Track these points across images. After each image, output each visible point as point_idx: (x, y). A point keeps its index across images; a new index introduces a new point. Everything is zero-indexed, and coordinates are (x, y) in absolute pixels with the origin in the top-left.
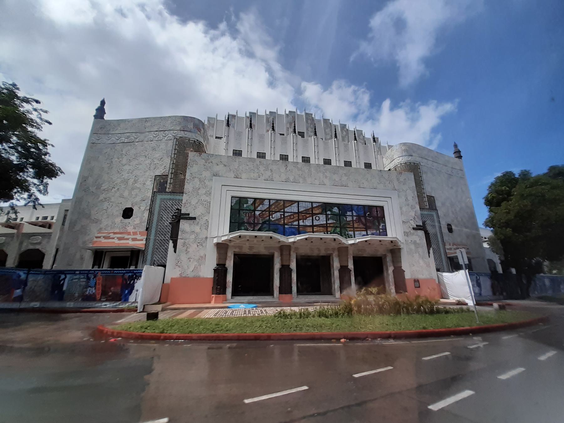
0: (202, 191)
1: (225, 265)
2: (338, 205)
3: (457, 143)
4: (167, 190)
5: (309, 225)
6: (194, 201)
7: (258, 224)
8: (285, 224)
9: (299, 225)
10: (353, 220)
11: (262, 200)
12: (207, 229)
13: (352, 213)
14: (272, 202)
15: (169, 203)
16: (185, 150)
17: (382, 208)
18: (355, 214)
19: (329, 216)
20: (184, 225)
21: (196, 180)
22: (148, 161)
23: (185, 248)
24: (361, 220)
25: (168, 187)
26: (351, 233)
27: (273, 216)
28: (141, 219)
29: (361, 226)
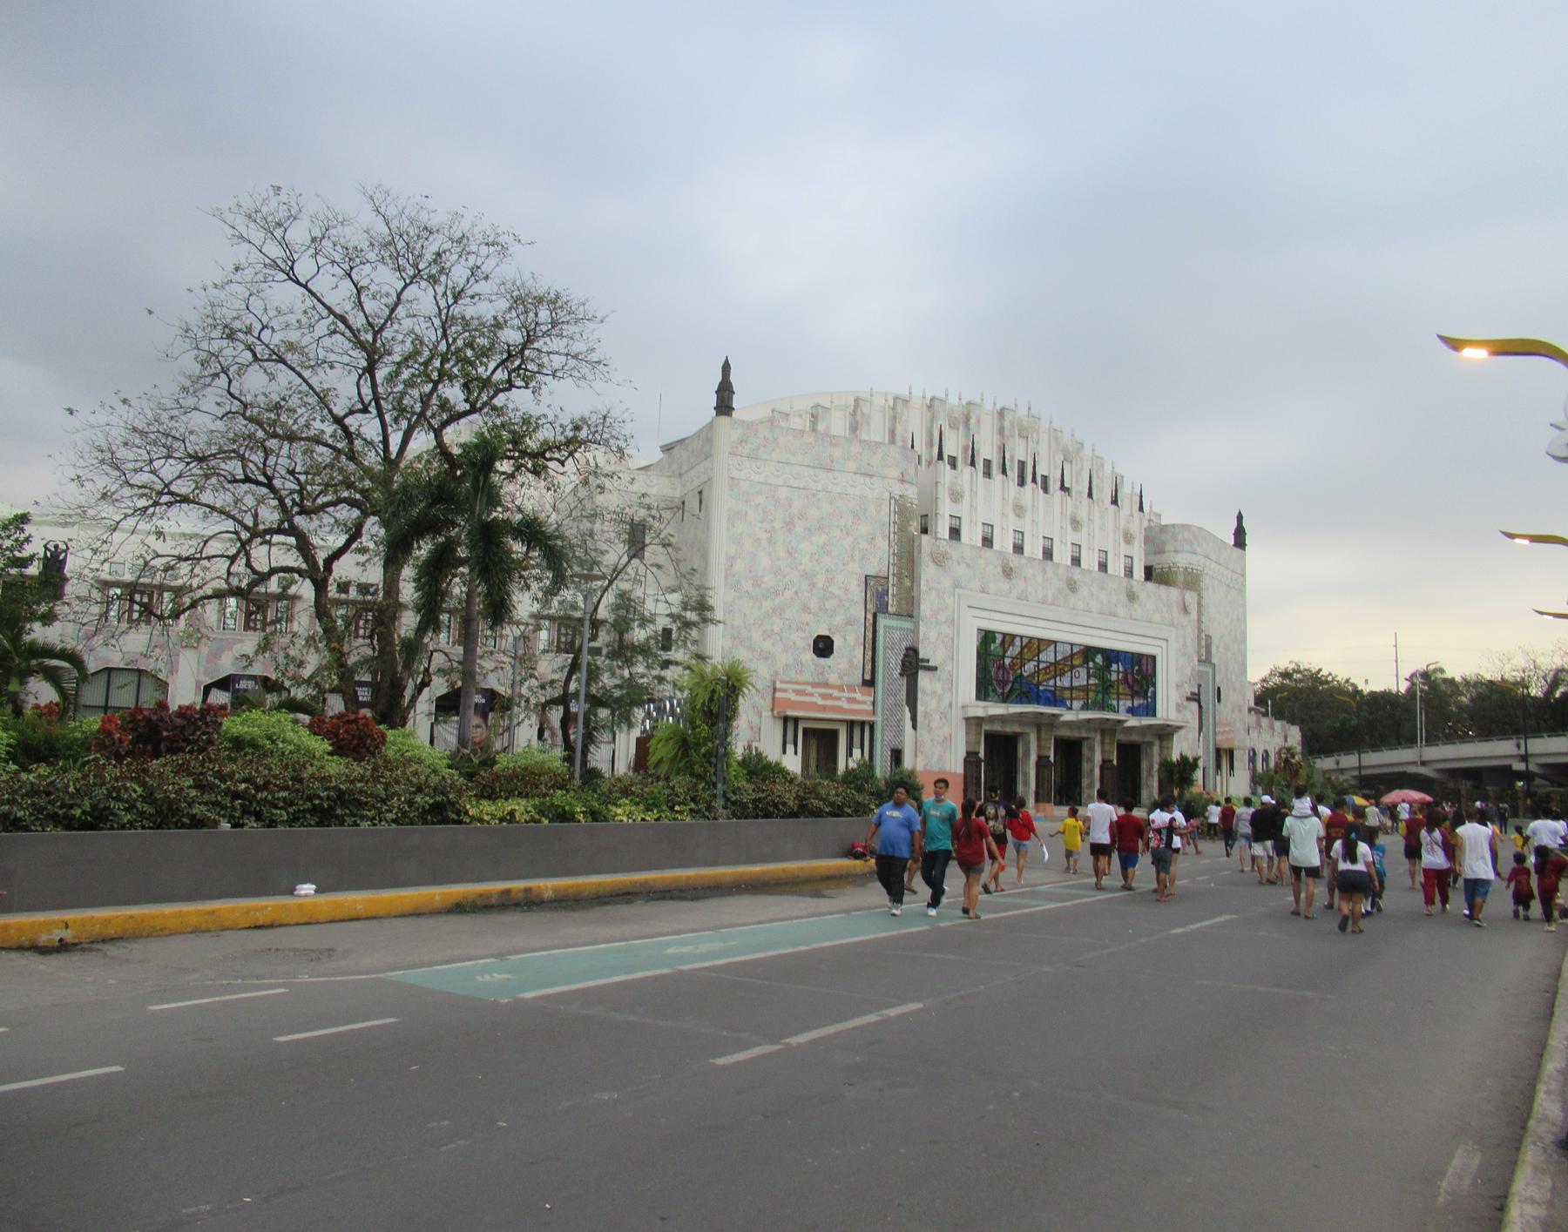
0: (943, 616)
6: (933, 636)
8: (1039, 683)
11: (1013, 636)
12: (951, 690)
14: (1025, 641)
15: (897, 634)
17: (1154, 658)
20: (924, 679)
22: (848, 542)
28: (851, 662)
29: (1128, 691)
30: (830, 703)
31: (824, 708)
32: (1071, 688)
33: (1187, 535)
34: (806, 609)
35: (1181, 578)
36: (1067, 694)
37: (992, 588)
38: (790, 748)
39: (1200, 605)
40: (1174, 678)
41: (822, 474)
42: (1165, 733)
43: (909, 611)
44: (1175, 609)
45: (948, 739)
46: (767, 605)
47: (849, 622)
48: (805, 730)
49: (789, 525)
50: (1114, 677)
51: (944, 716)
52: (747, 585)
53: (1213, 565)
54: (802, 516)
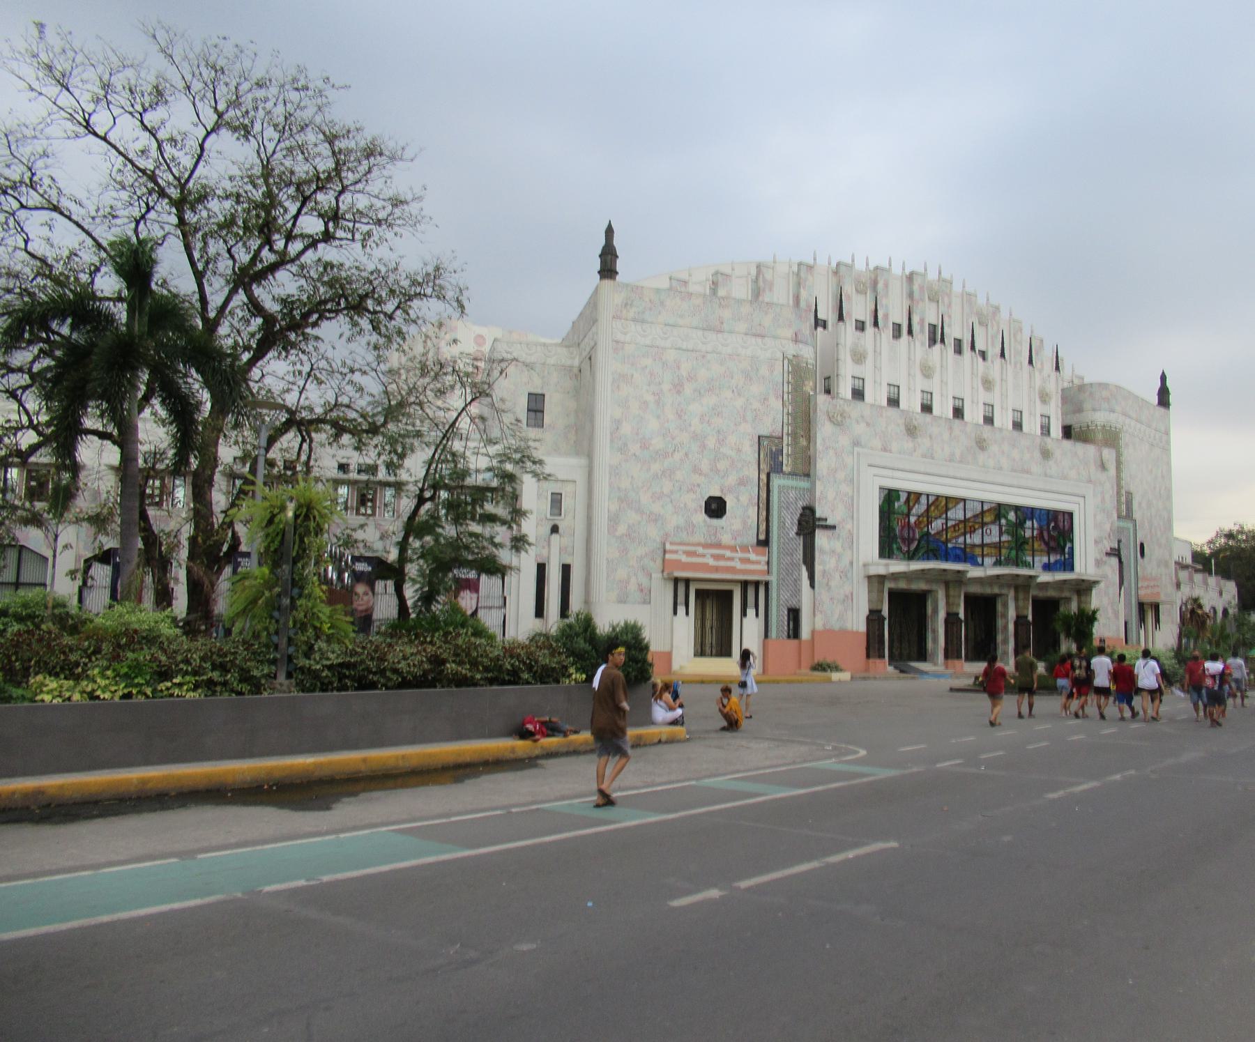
0: (841, 475)
2: (1017, 508)
4: (784, 468)
6: (831, 495)
7: (913, 539)
8: (947, 541)
11: (918, 495)
12: (851, 547)
14: (932, 499)
15: (792, 494)
18: (1036, 525)
20: (821, 538)
21: (831, 452)
22: (739, 403)
23: (825, 581)
25: (785, 462)
26: (1029, 559)
28: (744, 523)
29: (1043, 547)
30: (722, 563)
31: (717, 569)
32: (983, 545)
33: (1105, 393)
34: (696, 470)
35: (1100, 436)
36: (978, 551)
37: (895, 446)
38: (681, 609)
39: (1119, 464)
40: (1092, 534)
41: (711, 336)
42: (1083, 588)
43: (806, 470)
44: (1093, 469)
45: (849, 598)
46: (656, 467)
47: (742, 482)
48: (698, 592)
49: (678, 387)
50: (1028, 534)
51: (845, 574)
52: (634, 448)
53: (1133, 423)
54: (691, 378)
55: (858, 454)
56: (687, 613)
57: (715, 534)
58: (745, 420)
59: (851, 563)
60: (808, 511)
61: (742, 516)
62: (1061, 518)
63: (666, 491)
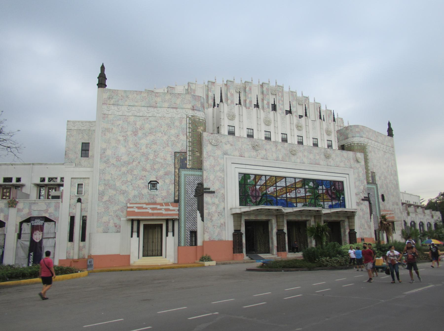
0: (217, 168)
1: (240, 230)
2: (313, 181)
3: (390, 122)
4: (188, 166)
5: (293, 197)
6: (212, 177)
7: (259, 196)
8: (277, 197)
9: (287, 197)
10: (323, 193)
11: (260, 176)
12: (224, 201)
13: (323, 187)
14: (268, 178)
15: (192, 178)
16: (197, 129)
17: (342, 182)
18: (324, 188)
19: (307, 190)
20: (207, 198)
21: (212, 158)
22: (165, 138)
23: (210, 217)
24: (328, 193)
25: (188, 163)
26: (322, 203)
27: (269, 189)
28: (168, 192)
29: (329, 198)
30: (155, 212)
31: (153, 214)
32: (296, 198)
33: (357, 130)
34: (144, 169)
35: (356, 148)
36: (294, 201)
37: (246, 154)
38: (135, 234)
39: (366, 160)
40: (354, 191)
41: (151, 109)
42: (351, 215)
44: (352, 161)
45: (223, 225)
46: (124, 169)
47: (166, 174)
48: (145, 226)
49: (135, 133)
51: (220, 214)
52: (113, 161)
53: (373, 142)
54: (141, 129)
55: (226, 158)
56: (138, 236)
57: (153, 199)
58: (168, 146)
59: (224, 208)
60: (201, 185)
61: (166, 189)
62: (337, 184)
63: (129, 179)
